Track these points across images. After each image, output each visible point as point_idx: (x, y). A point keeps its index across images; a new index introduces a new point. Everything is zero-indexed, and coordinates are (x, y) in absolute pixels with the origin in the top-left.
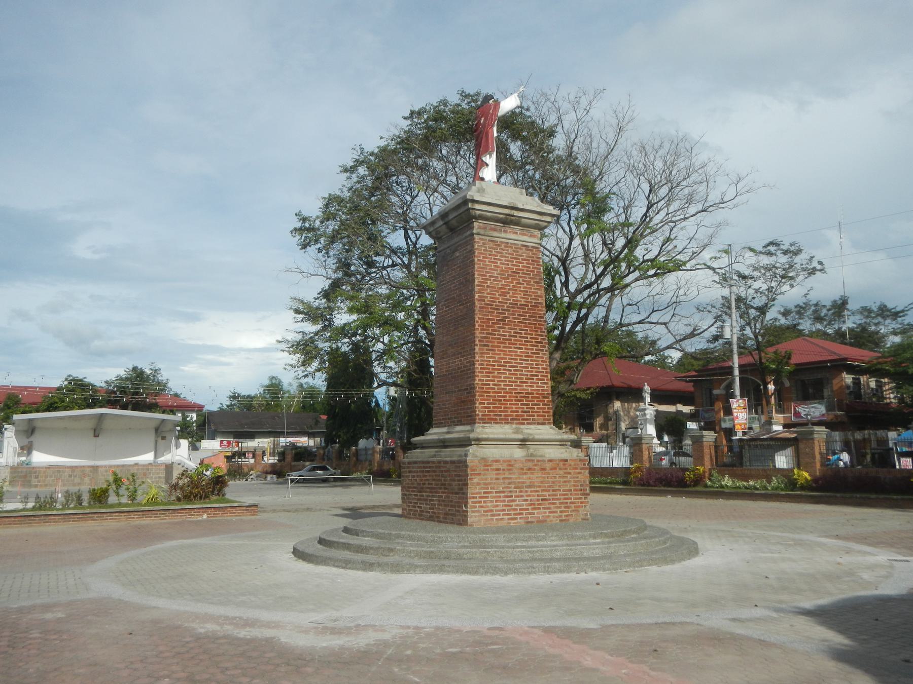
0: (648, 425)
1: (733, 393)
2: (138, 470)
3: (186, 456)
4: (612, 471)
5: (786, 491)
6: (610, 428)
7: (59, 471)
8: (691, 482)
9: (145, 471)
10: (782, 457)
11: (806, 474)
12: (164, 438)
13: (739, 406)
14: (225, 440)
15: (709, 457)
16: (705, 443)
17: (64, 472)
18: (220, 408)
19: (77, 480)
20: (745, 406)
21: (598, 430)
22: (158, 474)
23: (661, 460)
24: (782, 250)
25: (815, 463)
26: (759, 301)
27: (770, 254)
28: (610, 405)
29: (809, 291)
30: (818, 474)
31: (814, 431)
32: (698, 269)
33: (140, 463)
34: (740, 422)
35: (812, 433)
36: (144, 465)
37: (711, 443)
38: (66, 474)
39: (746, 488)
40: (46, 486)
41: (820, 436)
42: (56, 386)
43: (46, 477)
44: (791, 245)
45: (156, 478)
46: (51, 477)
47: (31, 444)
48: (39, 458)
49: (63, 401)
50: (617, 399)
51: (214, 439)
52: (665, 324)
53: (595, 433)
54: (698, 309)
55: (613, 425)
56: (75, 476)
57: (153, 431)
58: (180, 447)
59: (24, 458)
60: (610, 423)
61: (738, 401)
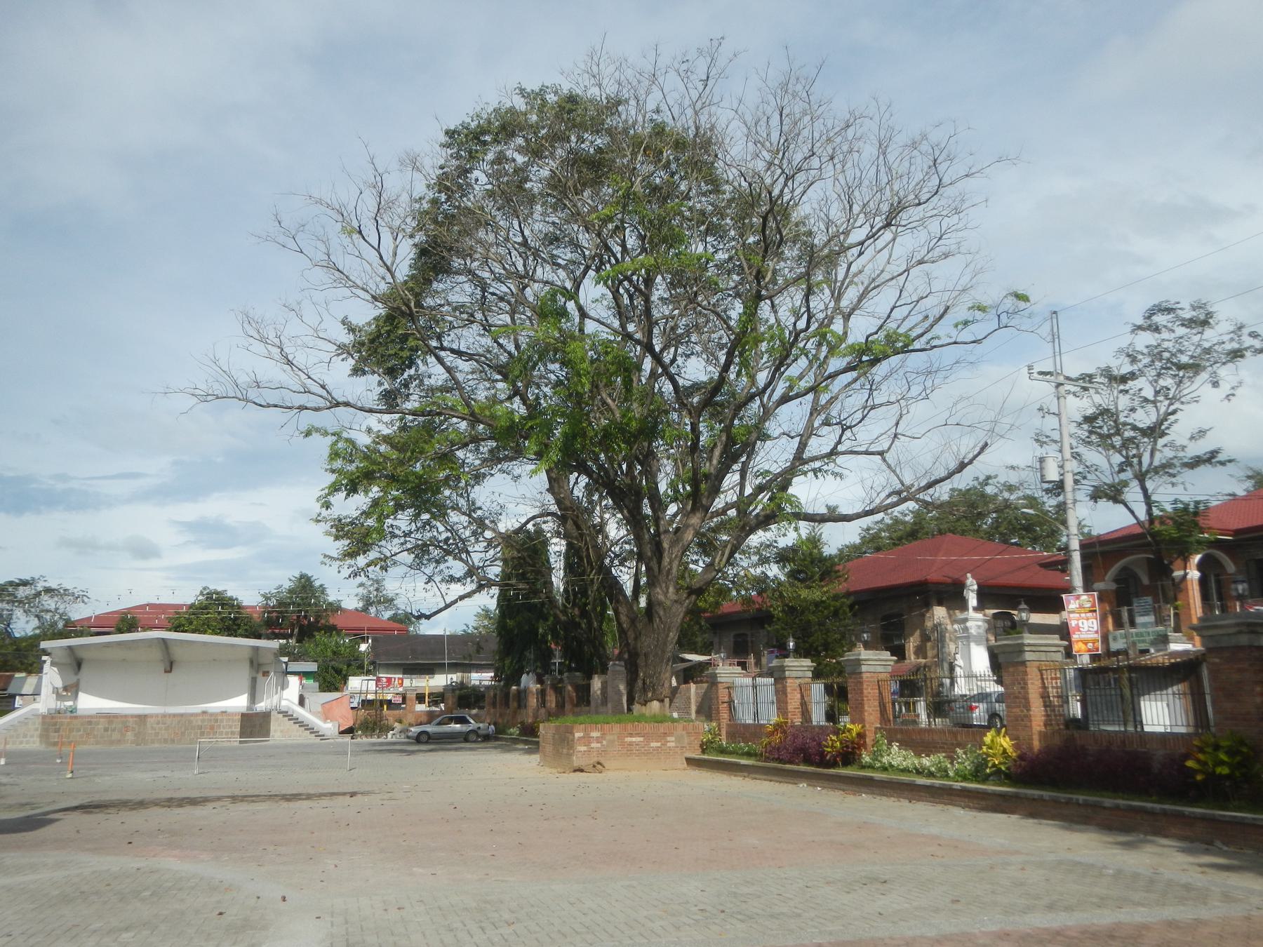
0: (973, 645)
1: (1070, 581)
2: (203, 721)
4: (754, 731)
5: (972, 781)
6: (930, 653)
7: (90, 723)
8: (835, 758)
10: (1153, 703)
11: (1005, 742)
13: (1081, 607)
14: (383, 676)
15: (877, 703)
16: (864, 676)
17: (98, 723)
18: (464, 631)
19: (116, 736)
20: (1093, 606)
21: (913, 657)
23: (971, 709)
24: (1184, 319)
25: (1028, 717)
26: (1145, 418)
27: (1156, 329)
28: (928, 615)
29: (1233, 388)
30: (1036, 744)
31: (1023, 645)
32: (935, 347)
34: (1084, 636)
35: (1020, 649)
36: (212, 715)
37: (883, 676)
39: (919, 772)
41: (1043, 656)
42: (190, 601)
43: (71, 730)
44: (1194, 308)
45: (227, 734)
46: (79, 730)
48: (88, 703)
49: (191, 623)
50: (940, 604)
52: (881, 453)
53: (907, 661)
54: (1037, 441)
55: (933, 648)
56: (114, 730)
57: (247, 665)
59: (70, 703)
60: (929, 644)
61: (1078, 597)
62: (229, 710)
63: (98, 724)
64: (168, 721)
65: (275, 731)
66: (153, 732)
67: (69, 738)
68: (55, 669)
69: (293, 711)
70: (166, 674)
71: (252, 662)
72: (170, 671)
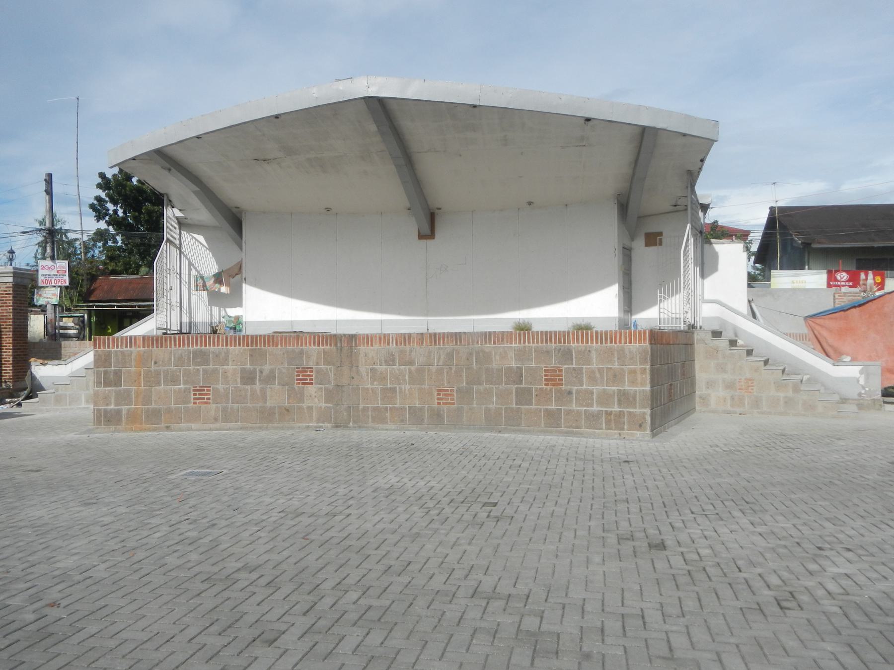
2: (521, 355)
3: (744, 309)
9: (553, 363)
12: (653, 239)
22: (616, 377)
33: (536, 328)
36: (548, 336)
38: (230, 368)
40: (154, 416)
43: (153, 379)
45: (605, 398)
46: (174, 380)
47: (239, 268)
51: (802, 268)
56: (270, 379)
58: (715, 269)
62: (599, 327)
63: (225, 362)
64: (419, 353)
65: (710, 384)
66: (376, 385)
67: (147, 400)
68: (201, 238)
69: (736, 331)
70: (423, 242)
71: (623, 206)
72: (431, 235)
